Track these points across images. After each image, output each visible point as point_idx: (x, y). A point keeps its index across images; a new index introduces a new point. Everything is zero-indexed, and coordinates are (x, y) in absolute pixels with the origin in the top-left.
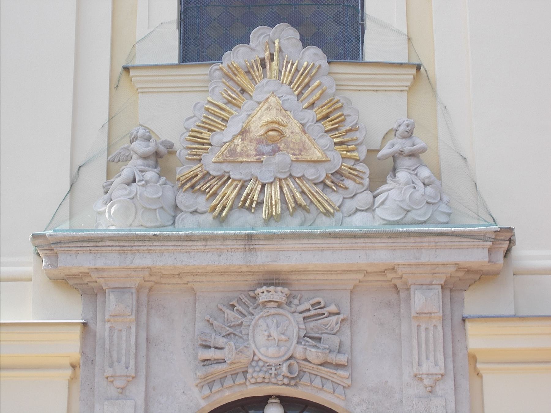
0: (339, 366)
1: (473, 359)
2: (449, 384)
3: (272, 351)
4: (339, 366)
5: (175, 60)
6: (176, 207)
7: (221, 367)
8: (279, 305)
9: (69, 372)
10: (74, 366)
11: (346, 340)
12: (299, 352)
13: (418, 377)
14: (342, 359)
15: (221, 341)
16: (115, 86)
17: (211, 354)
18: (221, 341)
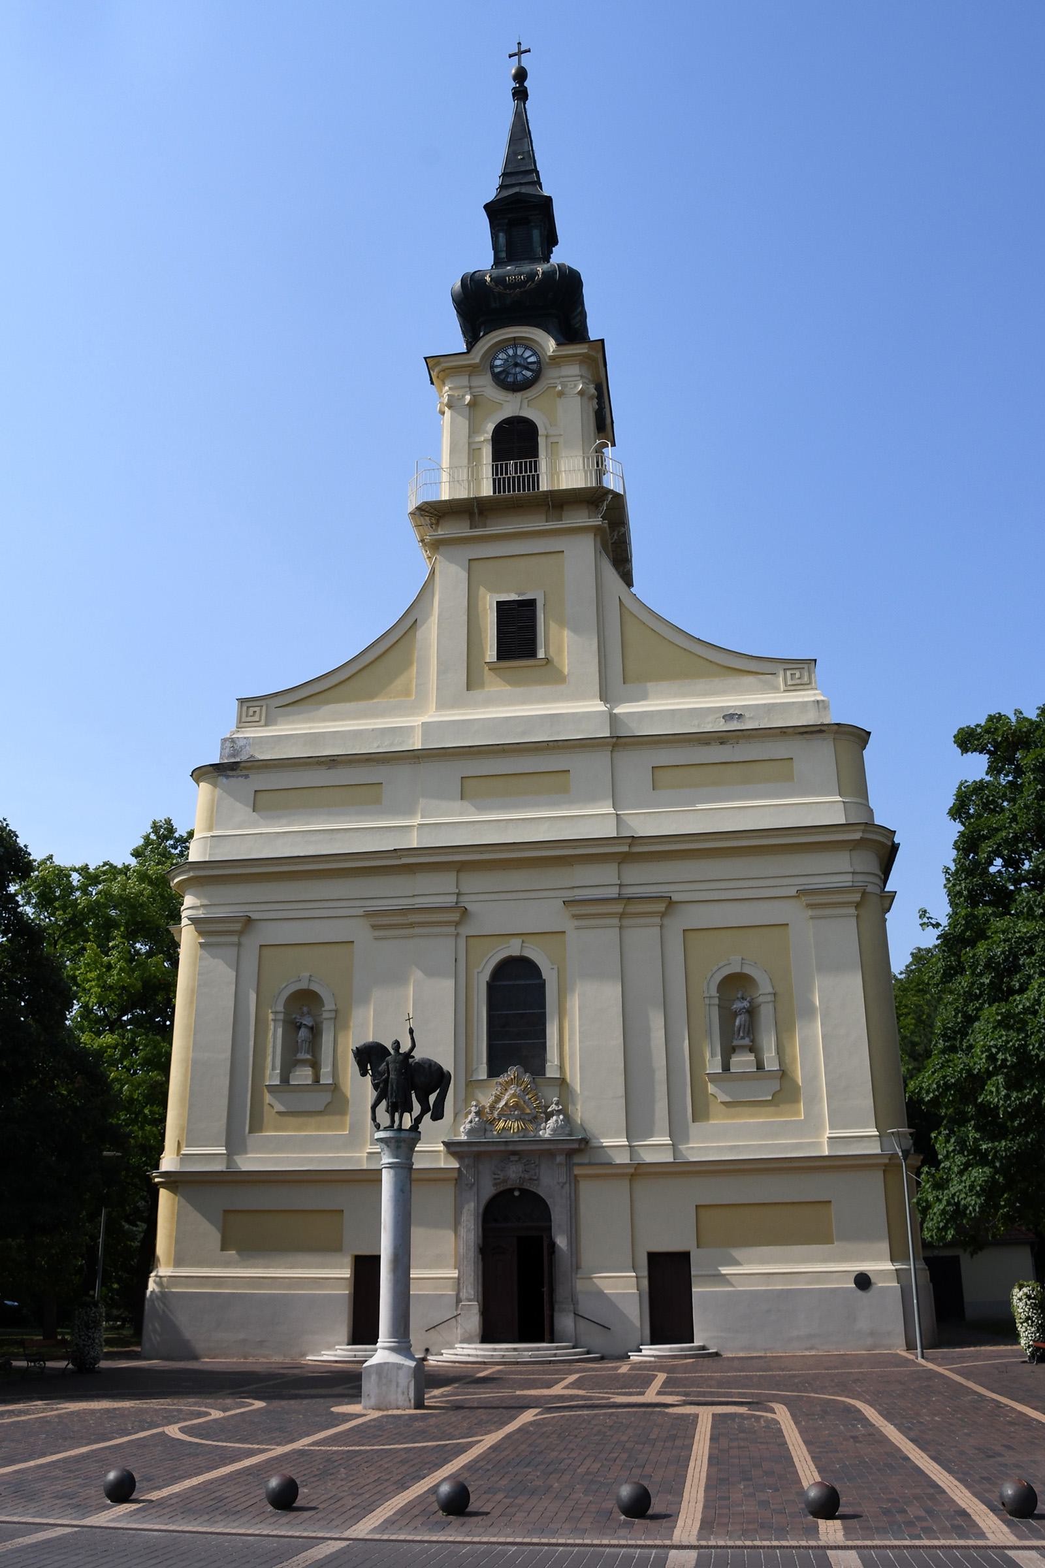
0: (536, 1180)
1: (576, 1176)
2: (568, 1185)
3: (514, 1175)
4: (536, 1180)
5: (485, 1077)
6: (485, 1130)
7: (498, 1181)
8: (517, 1161)
9: (454, 1182)
10: (456, 1180)
11: (537, 1171)
12: (523, 1176)
13: (558, 1183)
14: (535, 1178)
15: (499, 1172)
16: (467, 1085)
17: (496, 1176)
18: (499, 1172)
